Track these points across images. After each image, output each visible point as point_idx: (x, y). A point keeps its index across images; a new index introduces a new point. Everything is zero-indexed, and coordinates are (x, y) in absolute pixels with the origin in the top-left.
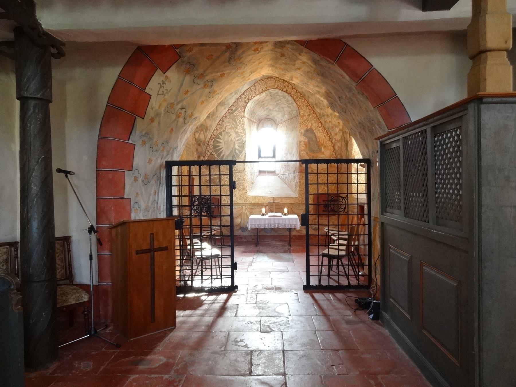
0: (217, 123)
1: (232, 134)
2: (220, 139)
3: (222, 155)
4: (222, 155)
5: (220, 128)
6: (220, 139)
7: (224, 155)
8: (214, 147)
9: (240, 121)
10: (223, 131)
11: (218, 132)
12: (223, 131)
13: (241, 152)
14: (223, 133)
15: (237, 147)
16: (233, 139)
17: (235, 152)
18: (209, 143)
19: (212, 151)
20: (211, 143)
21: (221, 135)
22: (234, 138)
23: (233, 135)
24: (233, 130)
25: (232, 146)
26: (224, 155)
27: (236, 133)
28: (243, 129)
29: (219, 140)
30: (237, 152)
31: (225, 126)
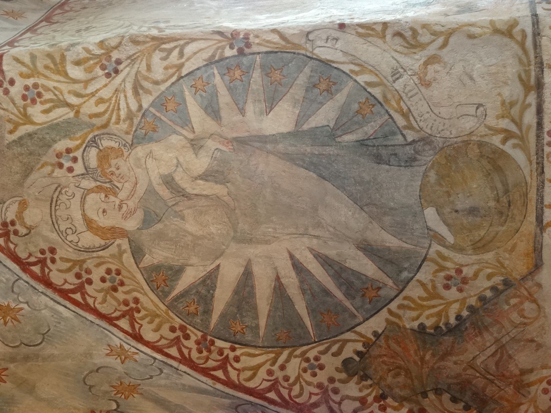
0: (66, 311)
1: (156, 171)
2: (209, 281)
3: (368, 268)
4: (368, 268)
5: (114, 281)
6: (209, 281)
7: (368, 249)
8: (287, 335)
9: (33, 95)
10: (137, 253)
11: (149, 300)
12: (137, 253)
13: (326, 77)
14: (157, 255)
15: (279, 121)
16: (201, 163)
17: (331, 134)
18: (259, 382)
19: (331, 363)
20: (254, 365)
21: (178, 271)
22: (196, 145)
23: (164, 159)
24: (123, 165)
25: (267, 166)
26: (368, 249)
27: (145, 131)
28: (107, 61)
29: (222, 297)
30: (325, 116)
31: (89, 239)
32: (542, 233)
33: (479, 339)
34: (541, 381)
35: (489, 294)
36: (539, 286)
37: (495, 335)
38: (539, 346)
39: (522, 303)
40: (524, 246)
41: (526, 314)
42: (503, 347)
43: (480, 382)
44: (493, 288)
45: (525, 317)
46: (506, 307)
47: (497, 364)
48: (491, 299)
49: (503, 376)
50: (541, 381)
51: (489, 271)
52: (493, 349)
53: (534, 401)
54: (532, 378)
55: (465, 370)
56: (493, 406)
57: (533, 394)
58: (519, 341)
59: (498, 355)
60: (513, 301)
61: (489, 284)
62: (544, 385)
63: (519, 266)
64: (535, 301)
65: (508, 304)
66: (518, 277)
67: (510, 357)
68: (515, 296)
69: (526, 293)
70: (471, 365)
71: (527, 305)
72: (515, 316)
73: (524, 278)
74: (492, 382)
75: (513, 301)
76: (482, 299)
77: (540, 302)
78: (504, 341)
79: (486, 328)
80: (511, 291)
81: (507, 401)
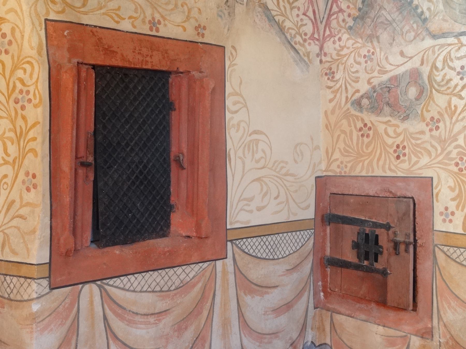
32: (454, 36)
33: (395, 10)
34: (374, 48)
35: (419, 11)
36: (423, 39)
37: (397, 19)
38: (391, 44)
39: (414, 31)
40: (446, 26)
41: (408, 34)
42: (391, 24)
43: (372, 14)
44: (422, 13)
45: (406, 34)
46: (412, 22)
47: (382, 22)
48: (416, 12)
49: (376, 27)
50: (374, 48)
51: (432, 9)
52: (390, 19)
53: (364, 46)
54: (375, 43)
55: (379, 5)
56: (361, 24)
57: (367, 44)
58: (394, 32)
59: (386, 22)
60: (415, 26)
61: (425, 10)
62: (372, 50)
63: (434, 26)
64: (415, 38)
65: (413, 23)
66: (428, 26)
67: (385, 29)
68: (418, 26)
69: (419, 32)
70: (381, 8)
71: (413, 34)
72: (407, 28)
73: (427, 29)
74: (373, 21)
75: (415, 26)
76: (417, 7)
77: (415, 41)
78: (394, 24)
79: (401, 13)
80: (420, 23)
81: (364, 31)
